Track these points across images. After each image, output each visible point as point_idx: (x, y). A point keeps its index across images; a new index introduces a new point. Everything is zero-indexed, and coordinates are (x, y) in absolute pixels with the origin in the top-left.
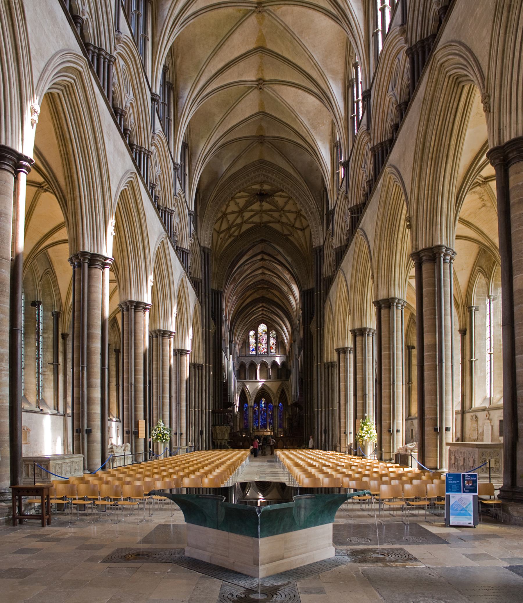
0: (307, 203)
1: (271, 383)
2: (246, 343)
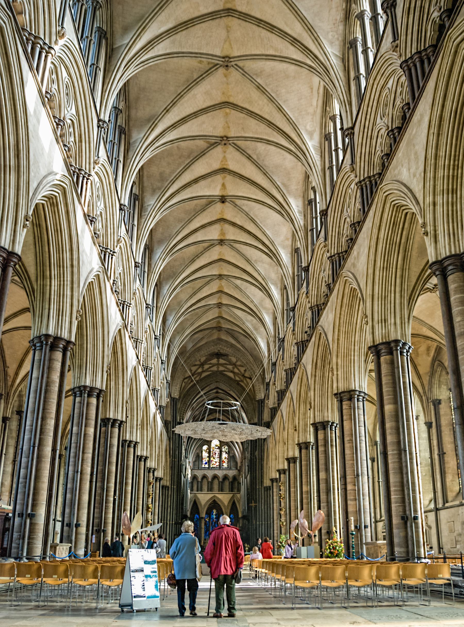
0: (252, 369)
1: (223, 495)
2: (199, 456)
